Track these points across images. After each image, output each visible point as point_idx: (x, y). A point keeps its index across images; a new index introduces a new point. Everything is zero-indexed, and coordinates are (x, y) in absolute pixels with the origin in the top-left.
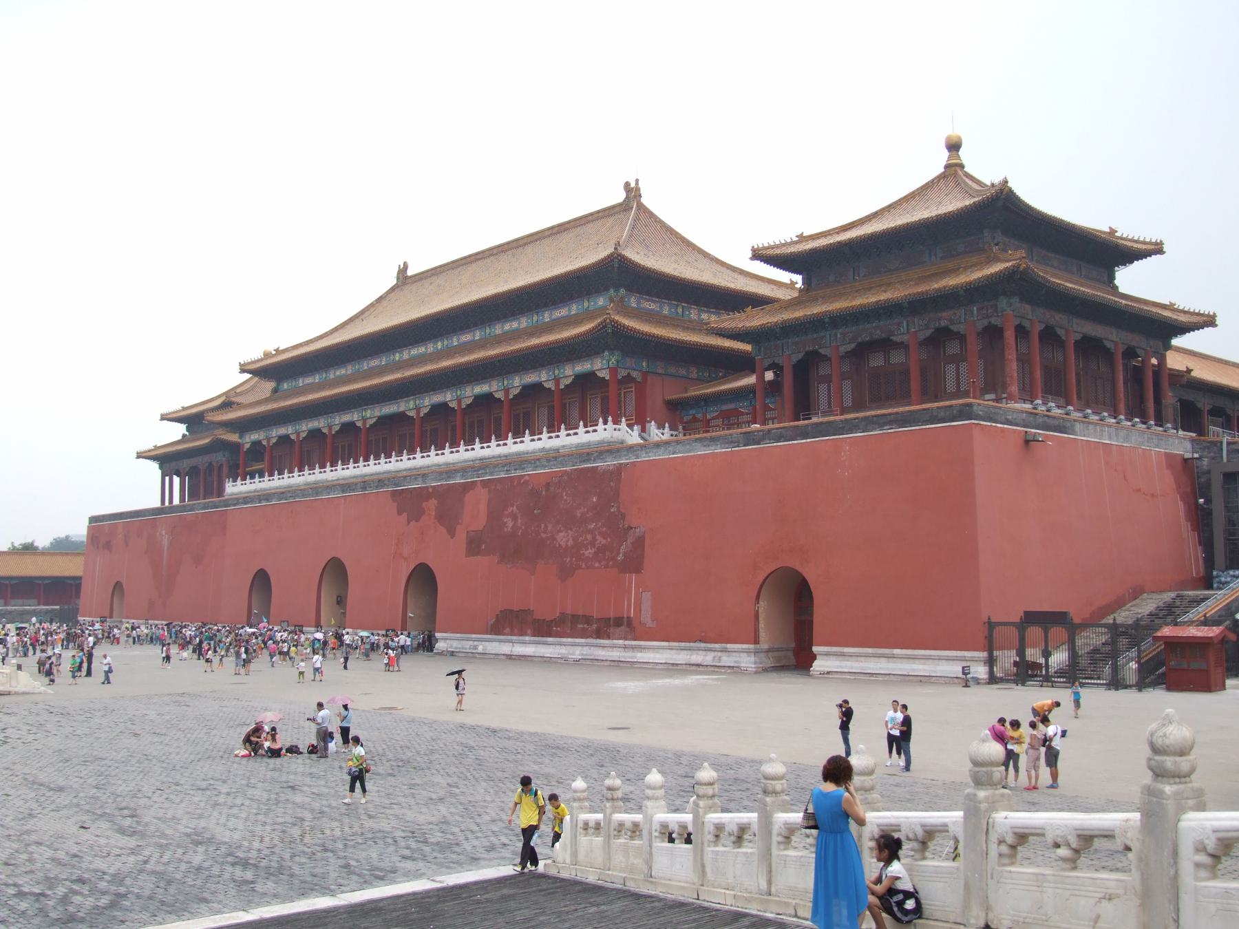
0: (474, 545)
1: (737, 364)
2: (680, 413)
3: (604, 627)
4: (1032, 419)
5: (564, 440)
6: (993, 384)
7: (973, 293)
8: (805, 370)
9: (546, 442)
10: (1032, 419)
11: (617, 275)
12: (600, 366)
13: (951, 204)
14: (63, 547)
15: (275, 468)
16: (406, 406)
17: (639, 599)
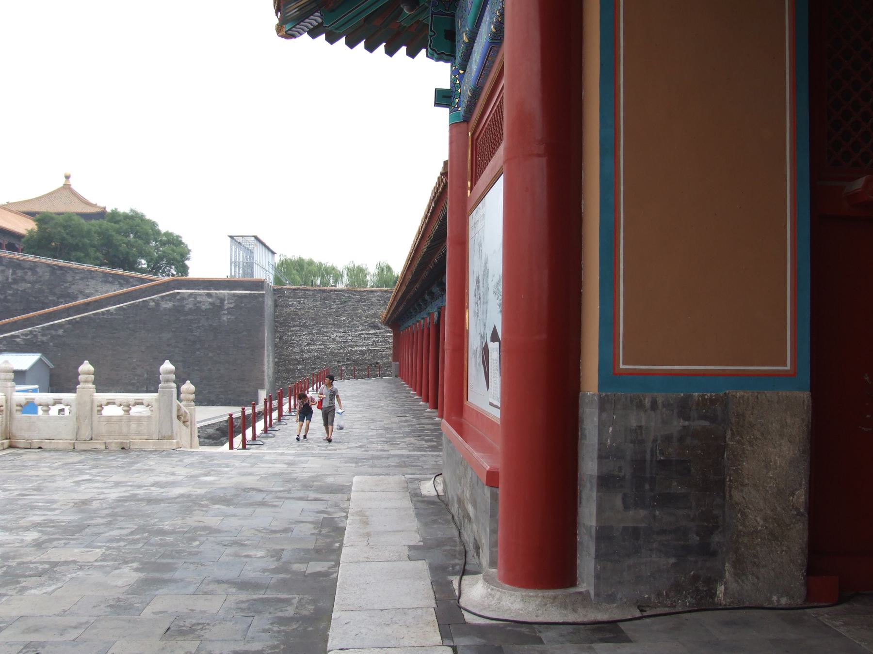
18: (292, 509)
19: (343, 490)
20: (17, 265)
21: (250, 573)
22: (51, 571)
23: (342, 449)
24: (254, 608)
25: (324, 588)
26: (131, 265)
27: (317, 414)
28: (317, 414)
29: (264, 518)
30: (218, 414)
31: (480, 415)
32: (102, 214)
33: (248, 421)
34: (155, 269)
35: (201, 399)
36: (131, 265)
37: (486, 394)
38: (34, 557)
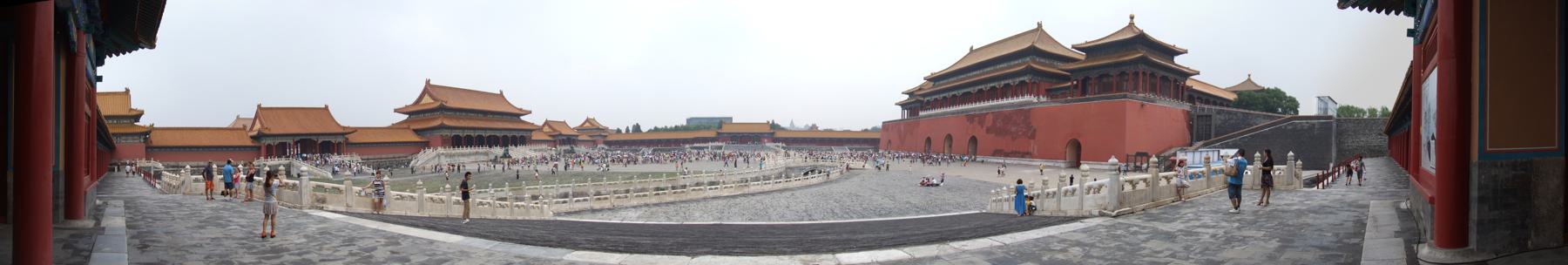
0: (988, 131)
1: (1066, 78)
2: (1050, 93)
3: (1024, 155)
4: (1144, 99)
5: (1015, 100)
6: (1136, 88)
7: (1131, 62)
8: (1085, 82)
9: (1010, 101)
10: (1144, 99)
11: (1033, 51)
12: (1026, 78)
13: (1129, 35)
14: (875, 129)
15: (933, 108)
16: (970, 90)
17: (1033, 147)
18: (1344, 215)
19: (1367, 206)
20: (1230, 113)
21: (1325, 243)
22: (1244, 240)
23: (1366, 189)
24: (1327, 259)
25: (1357, 250)
26: (1275, 111)
27: (1355, 174)
28: (1355, 174)
29: (1331, 219)
30: (1308, 174)
31: (1426, 172)
32: (1263, 90)
33: (1325, 177)
34: (1285, 112)
35: (1305, 168)
36: (1275, 111)
37: (1429, 163)
38: (1237, 233)
